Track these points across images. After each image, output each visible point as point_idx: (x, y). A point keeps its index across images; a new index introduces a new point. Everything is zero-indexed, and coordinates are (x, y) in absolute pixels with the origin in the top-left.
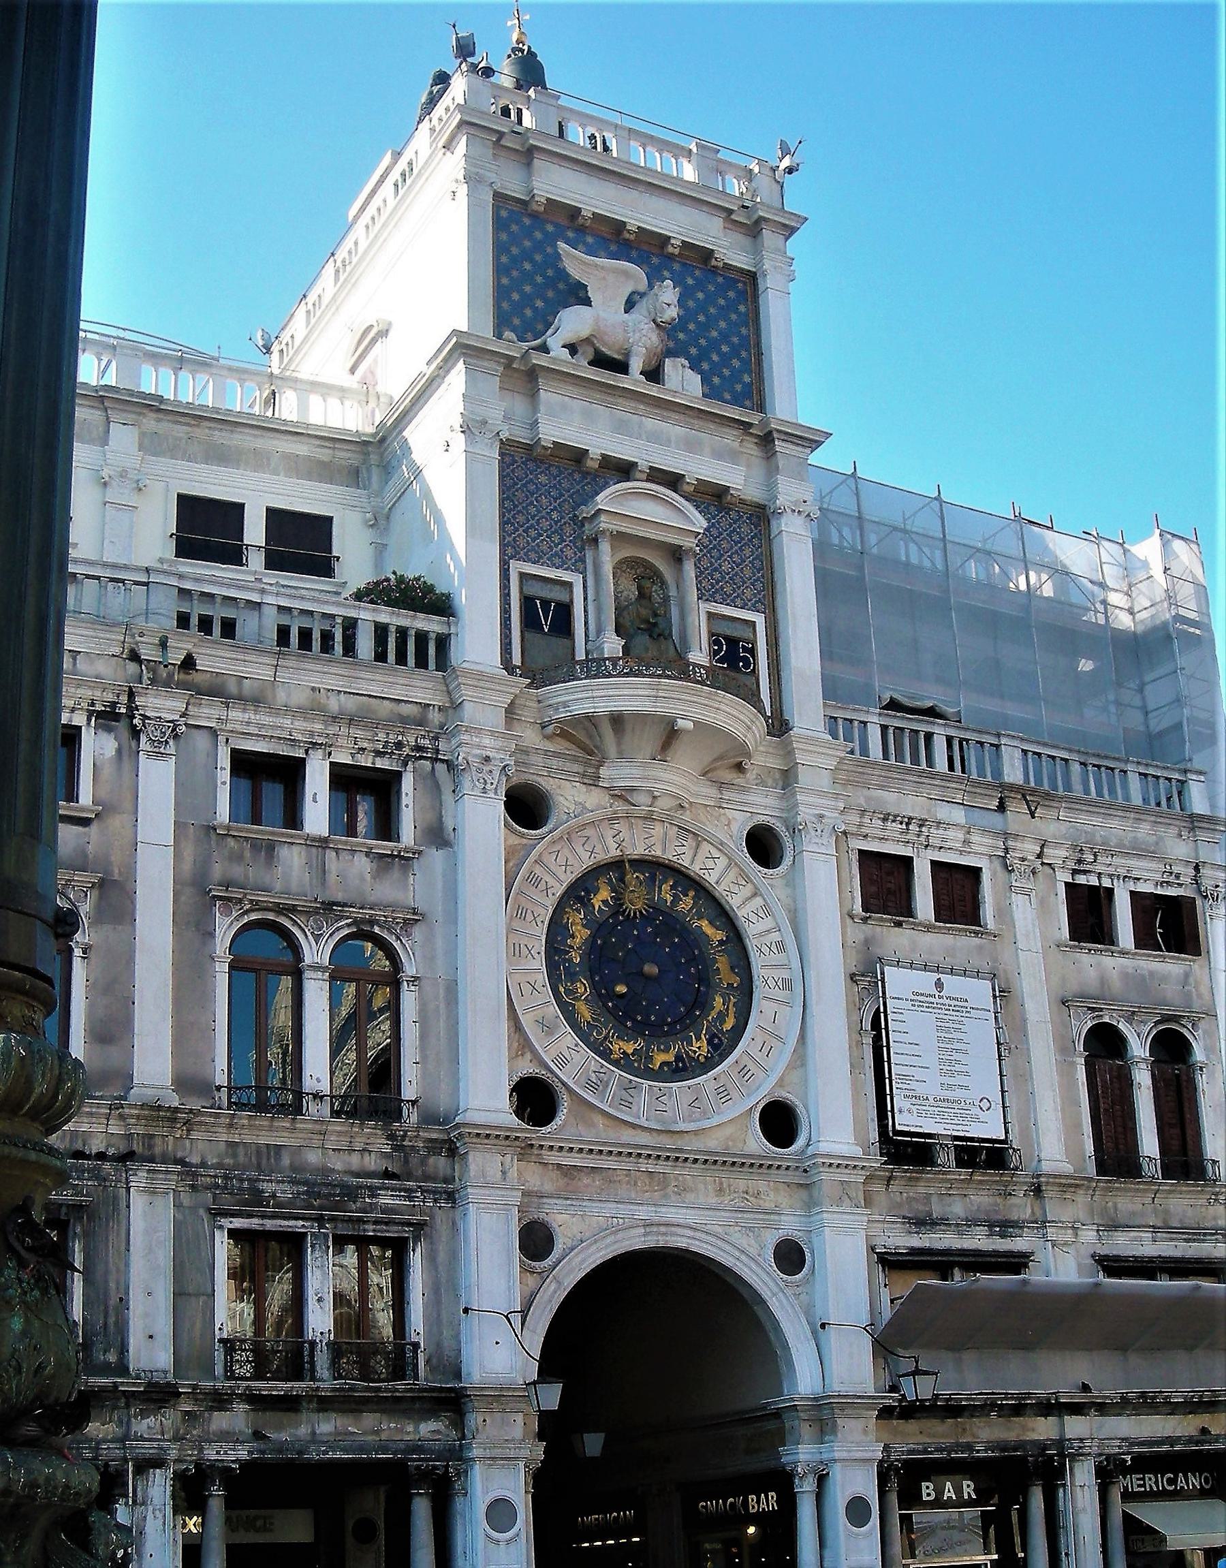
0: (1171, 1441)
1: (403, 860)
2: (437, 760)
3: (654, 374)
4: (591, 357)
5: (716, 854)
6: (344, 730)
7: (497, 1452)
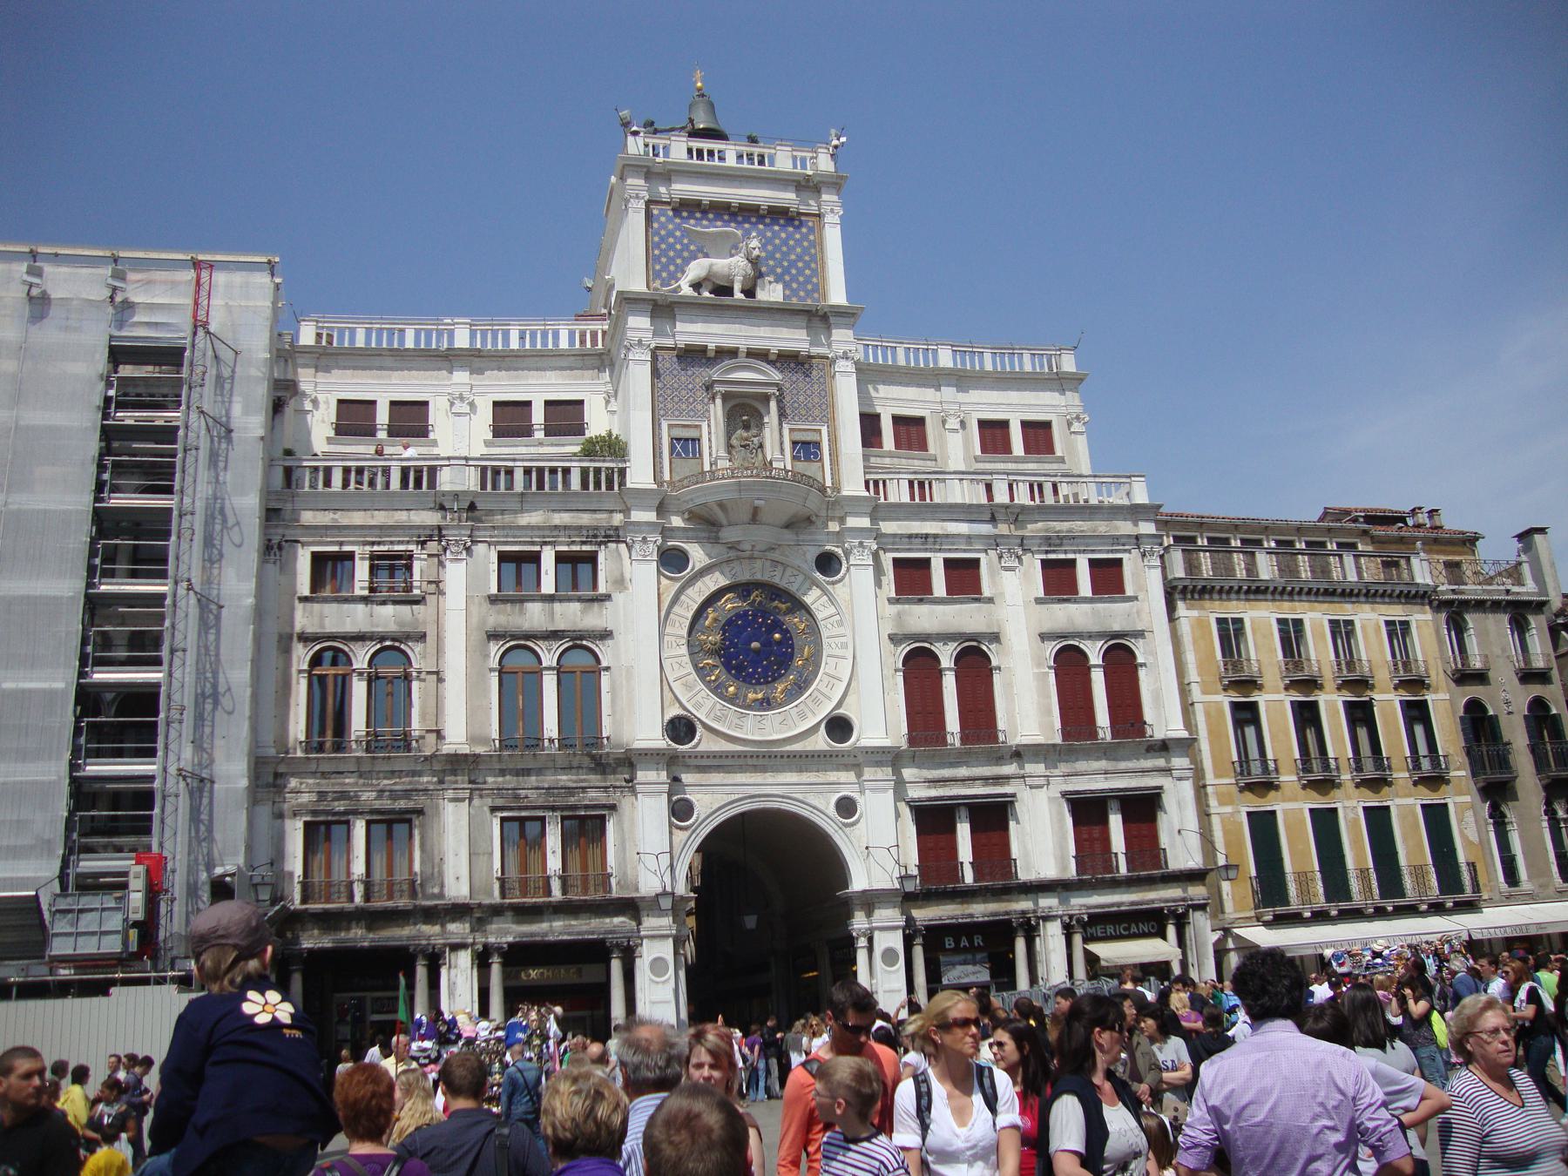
0: (1119, 904)
2: (618, 542)
3: (749, 292)
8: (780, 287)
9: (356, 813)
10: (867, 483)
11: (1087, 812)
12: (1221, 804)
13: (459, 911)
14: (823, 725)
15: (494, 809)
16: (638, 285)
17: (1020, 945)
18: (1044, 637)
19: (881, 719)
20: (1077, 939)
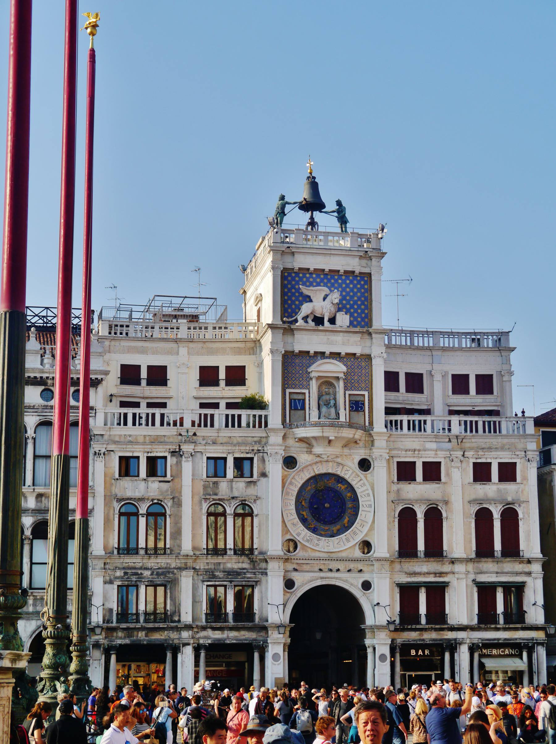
0: (498, 639)
1: (254, 483)
3: (332, 321)
4: (312, 318)
5: (348, 469)
6: (237, 448)
7: (274, 641)
9: (141, 581)
10: (386, 421)
11: (486, 592)
13: (188, 627)
14: (357, 545)
15: (203, 581)
17: (447, 656)
18: (470, 502)
20: (476, 656)
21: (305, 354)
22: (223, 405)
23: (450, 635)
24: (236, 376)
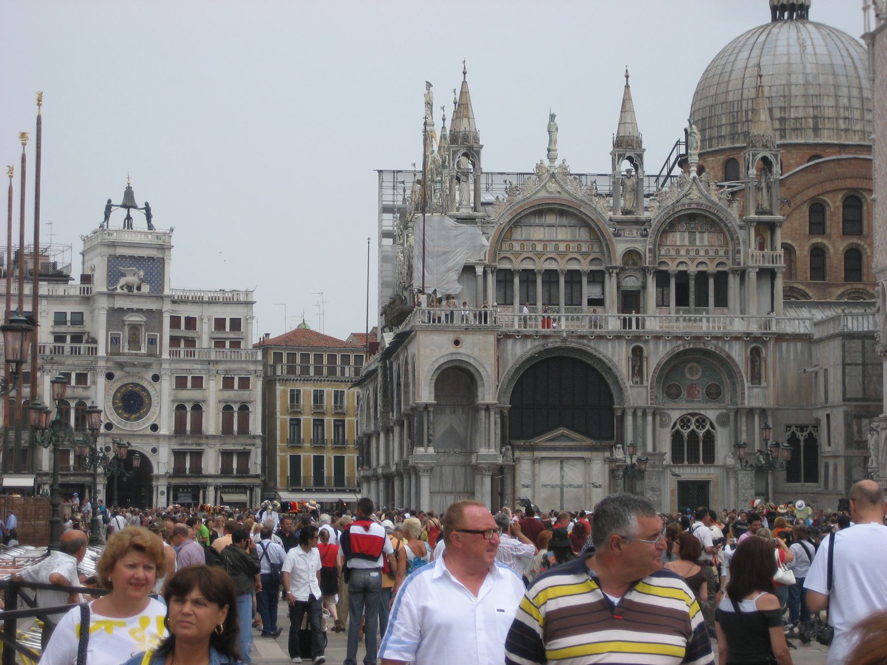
1: (88, 388)
3: (139, 288)
8: (148, 286)
11: (226, 455)
12: (281, 451)
16: (104, 290)
18: (220, 402)
19: (166, 427)
20: (219, 492)
21: (121, 310)
22: (68, 338)
23: (203, 481)
24: (78, 318)
